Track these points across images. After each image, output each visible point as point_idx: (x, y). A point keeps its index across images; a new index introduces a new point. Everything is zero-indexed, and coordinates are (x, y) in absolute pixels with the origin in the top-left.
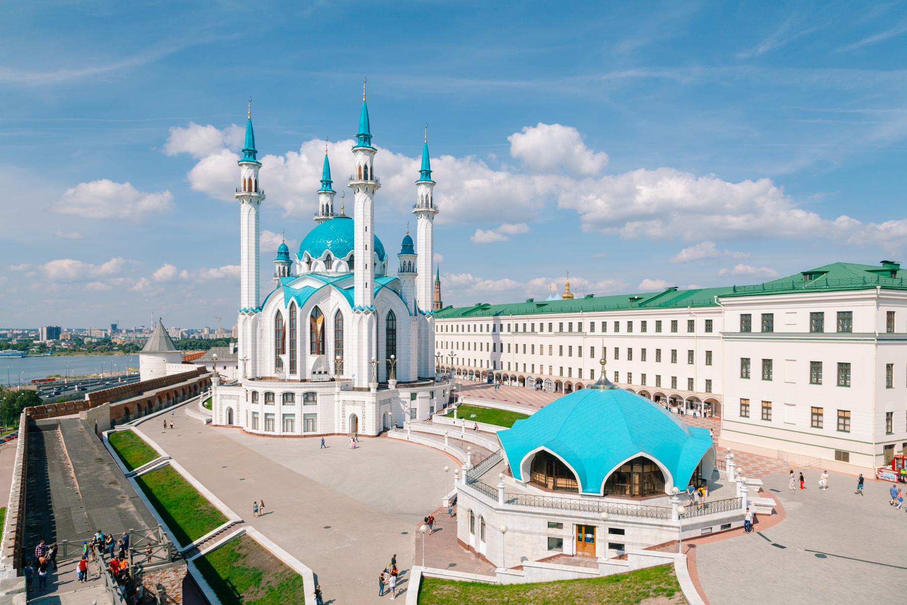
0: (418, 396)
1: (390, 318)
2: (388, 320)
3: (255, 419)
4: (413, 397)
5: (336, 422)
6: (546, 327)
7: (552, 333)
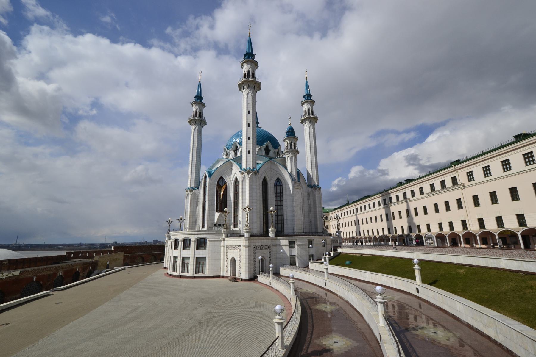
0: (297, 243)
1: (278, 184)
2: (276, 186)
3: (175, 262)
4: (292, 244)
5: (222, 265)
6: (417, 192)
7: (425, 195)
